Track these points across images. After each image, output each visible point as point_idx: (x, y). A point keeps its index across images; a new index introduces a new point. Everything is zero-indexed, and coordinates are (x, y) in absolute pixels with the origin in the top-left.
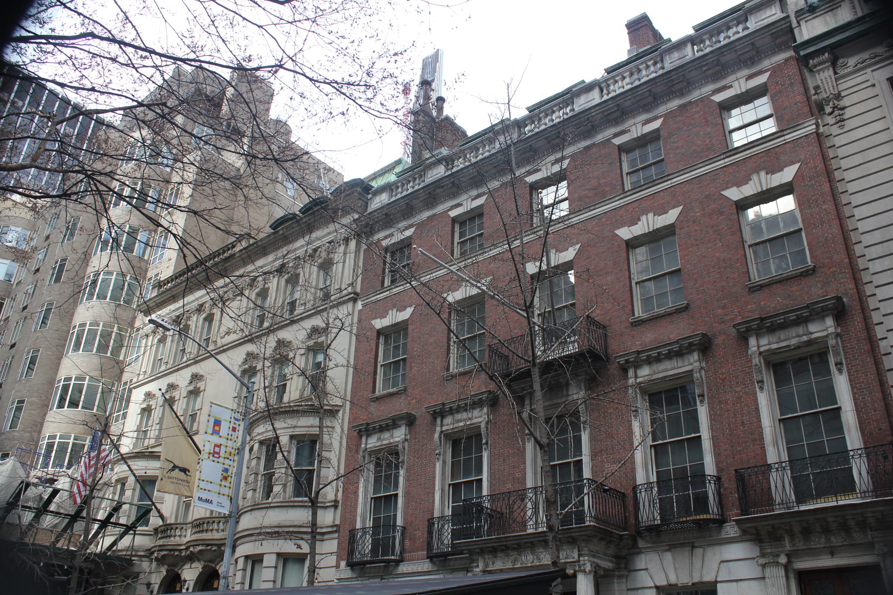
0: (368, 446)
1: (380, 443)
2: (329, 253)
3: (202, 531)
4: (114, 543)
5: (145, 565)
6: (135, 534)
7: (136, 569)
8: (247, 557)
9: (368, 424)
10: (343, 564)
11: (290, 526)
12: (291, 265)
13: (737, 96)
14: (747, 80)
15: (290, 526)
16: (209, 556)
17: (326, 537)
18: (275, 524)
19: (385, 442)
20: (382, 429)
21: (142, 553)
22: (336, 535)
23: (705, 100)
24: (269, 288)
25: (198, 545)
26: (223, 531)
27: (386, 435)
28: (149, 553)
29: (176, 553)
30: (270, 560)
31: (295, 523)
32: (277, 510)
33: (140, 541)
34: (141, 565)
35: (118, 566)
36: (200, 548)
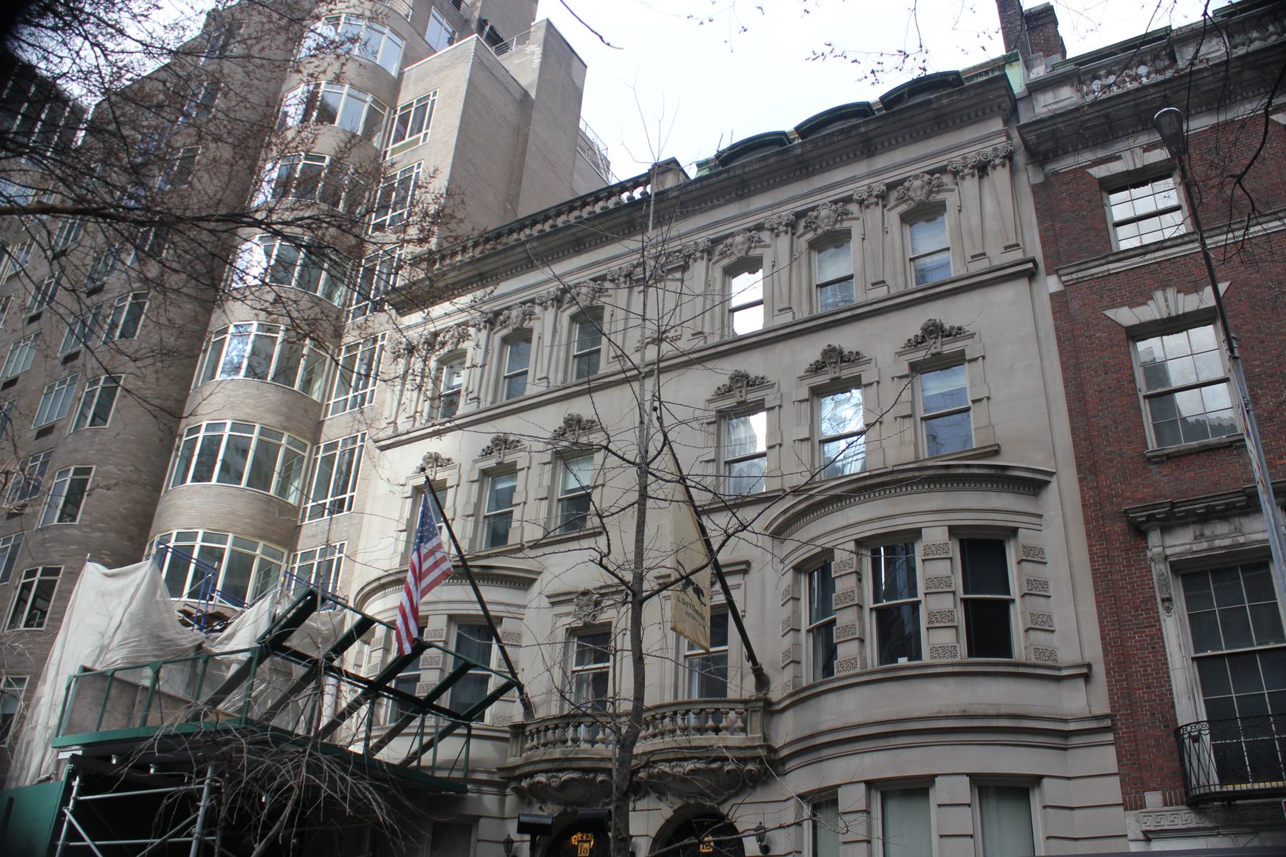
0: (1168, 552)
1: (1205, 545)
2: (930, 192)
3: (662, 734)
4: (416, 756)
5: (490, 802)
6: (469, 736)
7: (470, 810)
8: (870, 784)
9: (1173, 505)
12: (824, 213)
13: (1127, 173)
14: (1145, 151)
16: (700, 784)
17: (1075, 741)
18: (956, 710)
19: (1217, 543)
20: (1207, 517)
21: (484, 777)
22: (1110, 737)
23: (1081, 171)
24: (531, 331)
25: (685, 759)
26: (744, 730)
27: (1222, 528)
28: (507, 779)
29: (600, 778)
31: (1004, 711)
32: (950, 681)
33: (482, 751)
34: (479, 801)
36: (689, 766)
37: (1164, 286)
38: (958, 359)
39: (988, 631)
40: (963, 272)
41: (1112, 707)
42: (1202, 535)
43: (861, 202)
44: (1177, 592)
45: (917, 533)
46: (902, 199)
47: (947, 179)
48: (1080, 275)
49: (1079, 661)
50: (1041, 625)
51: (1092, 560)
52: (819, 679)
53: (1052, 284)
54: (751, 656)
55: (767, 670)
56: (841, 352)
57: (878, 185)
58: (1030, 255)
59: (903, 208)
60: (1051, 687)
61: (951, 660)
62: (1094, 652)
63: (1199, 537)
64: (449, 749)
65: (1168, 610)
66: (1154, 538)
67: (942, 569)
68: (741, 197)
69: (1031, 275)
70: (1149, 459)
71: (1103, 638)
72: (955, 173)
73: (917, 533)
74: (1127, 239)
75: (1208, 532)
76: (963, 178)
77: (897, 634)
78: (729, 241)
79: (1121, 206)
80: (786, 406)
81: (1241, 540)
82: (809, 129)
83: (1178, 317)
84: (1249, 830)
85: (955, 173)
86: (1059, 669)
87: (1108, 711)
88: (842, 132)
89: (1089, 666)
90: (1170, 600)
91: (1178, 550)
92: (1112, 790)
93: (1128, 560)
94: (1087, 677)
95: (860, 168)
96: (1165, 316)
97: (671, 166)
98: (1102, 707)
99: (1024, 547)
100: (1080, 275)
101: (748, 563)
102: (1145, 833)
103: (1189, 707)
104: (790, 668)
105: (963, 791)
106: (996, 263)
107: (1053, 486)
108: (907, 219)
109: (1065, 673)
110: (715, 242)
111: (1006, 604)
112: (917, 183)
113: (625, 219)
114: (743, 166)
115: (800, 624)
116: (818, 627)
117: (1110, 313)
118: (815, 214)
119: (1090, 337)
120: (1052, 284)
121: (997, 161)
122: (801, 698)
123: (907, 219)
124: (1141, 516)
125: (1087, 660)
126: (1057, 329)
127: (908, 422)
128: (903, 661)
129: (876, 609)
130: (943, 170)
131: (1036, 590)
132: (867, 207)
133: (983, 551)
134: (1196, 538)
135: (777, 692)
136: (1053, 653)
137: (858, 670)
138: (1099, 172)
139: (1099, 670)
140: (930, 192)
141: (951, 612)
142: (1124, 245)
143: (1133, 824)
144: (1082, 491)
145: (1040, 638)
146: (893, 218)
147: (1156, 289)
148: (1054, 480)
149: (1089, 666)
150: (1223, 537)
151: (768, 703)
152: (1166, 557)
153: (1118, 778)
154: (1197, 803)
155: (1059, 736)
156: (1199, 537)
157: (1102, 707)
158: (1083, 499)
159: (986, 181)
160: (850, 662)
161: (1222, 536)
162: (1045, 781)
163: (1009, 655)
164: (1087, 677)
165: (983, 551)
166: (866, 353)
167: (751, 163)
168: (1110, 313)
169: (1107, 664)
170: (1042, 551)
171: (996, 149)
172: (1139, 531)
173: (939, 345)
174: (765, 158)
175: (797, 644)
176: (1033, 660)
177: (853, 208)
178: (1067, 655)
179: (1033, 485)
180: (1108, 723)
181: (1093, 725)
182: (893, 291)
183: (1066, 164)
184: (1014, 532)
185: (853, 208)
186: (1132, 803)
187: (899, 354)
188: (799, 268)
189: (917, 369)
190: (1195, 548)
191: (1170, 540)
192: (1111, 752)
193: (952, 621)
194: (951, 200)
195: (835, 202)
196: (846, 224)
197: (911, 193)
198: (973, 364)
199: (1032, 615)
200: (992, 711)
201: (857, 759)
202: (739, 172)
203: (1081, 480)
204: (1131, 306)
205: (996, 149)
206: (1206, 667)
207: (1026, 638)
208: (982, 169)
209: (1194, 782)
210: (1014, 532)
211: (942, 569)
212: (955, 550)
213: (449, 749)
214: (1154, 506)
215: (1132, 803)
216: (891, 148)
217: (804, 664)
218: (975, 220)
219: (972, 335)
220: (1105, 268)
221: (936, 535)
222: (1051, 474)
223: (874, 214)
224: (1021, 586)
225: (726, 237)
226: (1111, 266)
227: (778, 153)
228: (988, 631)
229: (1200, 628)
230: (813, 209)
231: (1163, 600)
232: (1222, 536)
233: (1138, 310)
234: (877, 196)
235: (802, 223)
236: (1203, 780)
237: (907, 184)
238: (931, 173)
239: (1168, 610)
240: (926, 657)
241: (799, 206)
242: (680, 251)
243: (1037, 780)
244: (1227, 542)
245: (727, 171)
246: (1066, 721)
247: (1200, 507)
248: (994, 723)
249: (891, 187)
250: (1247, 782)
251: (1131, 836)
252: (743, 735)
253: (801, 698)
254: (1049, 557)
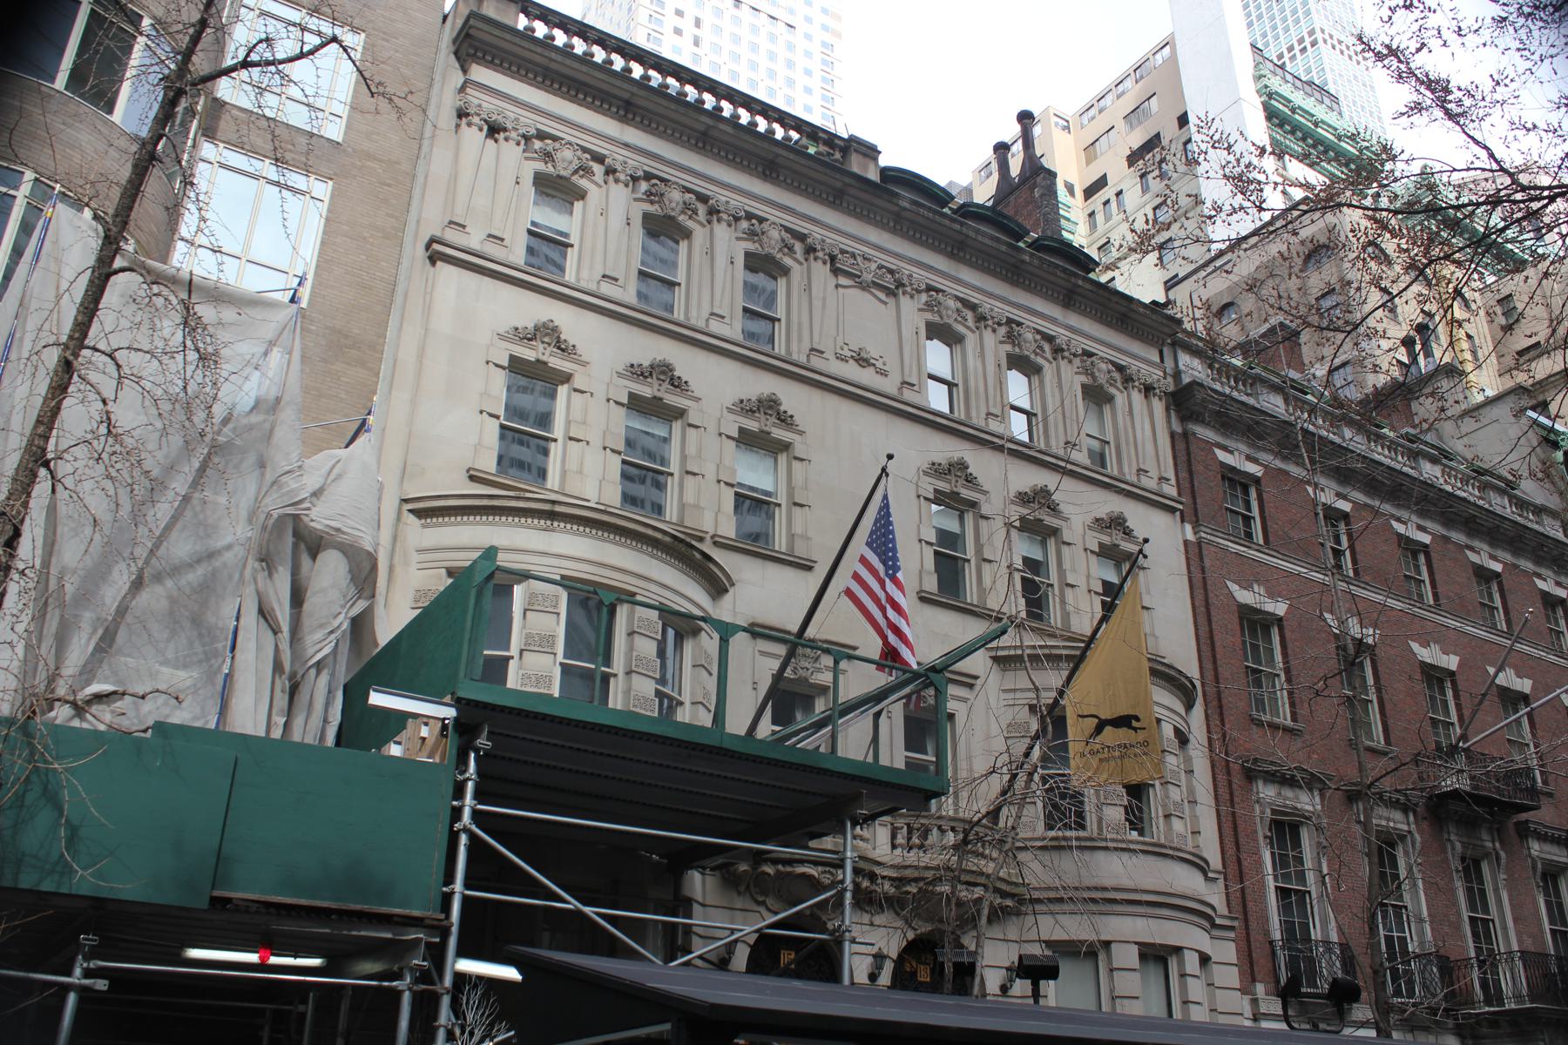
22: (1232, 935)
68: (952, 256)
85: (610, 171)
88: (1064, 270)
97: (871, 152)
101: (976, 678)
110: (929, 288)
112: (1103, 366)
113: (839, 185)
114: (977, 231)
138: (1222, 456)
167: (984, 234)
174: (998, 240)
183: (1204, 433)
201: (1129, 920)
202: (971, 234)
216: (1083, 312)
225: (938, 291)
227: (1010, 245)
242: (891, 272)
245: (962, 224)
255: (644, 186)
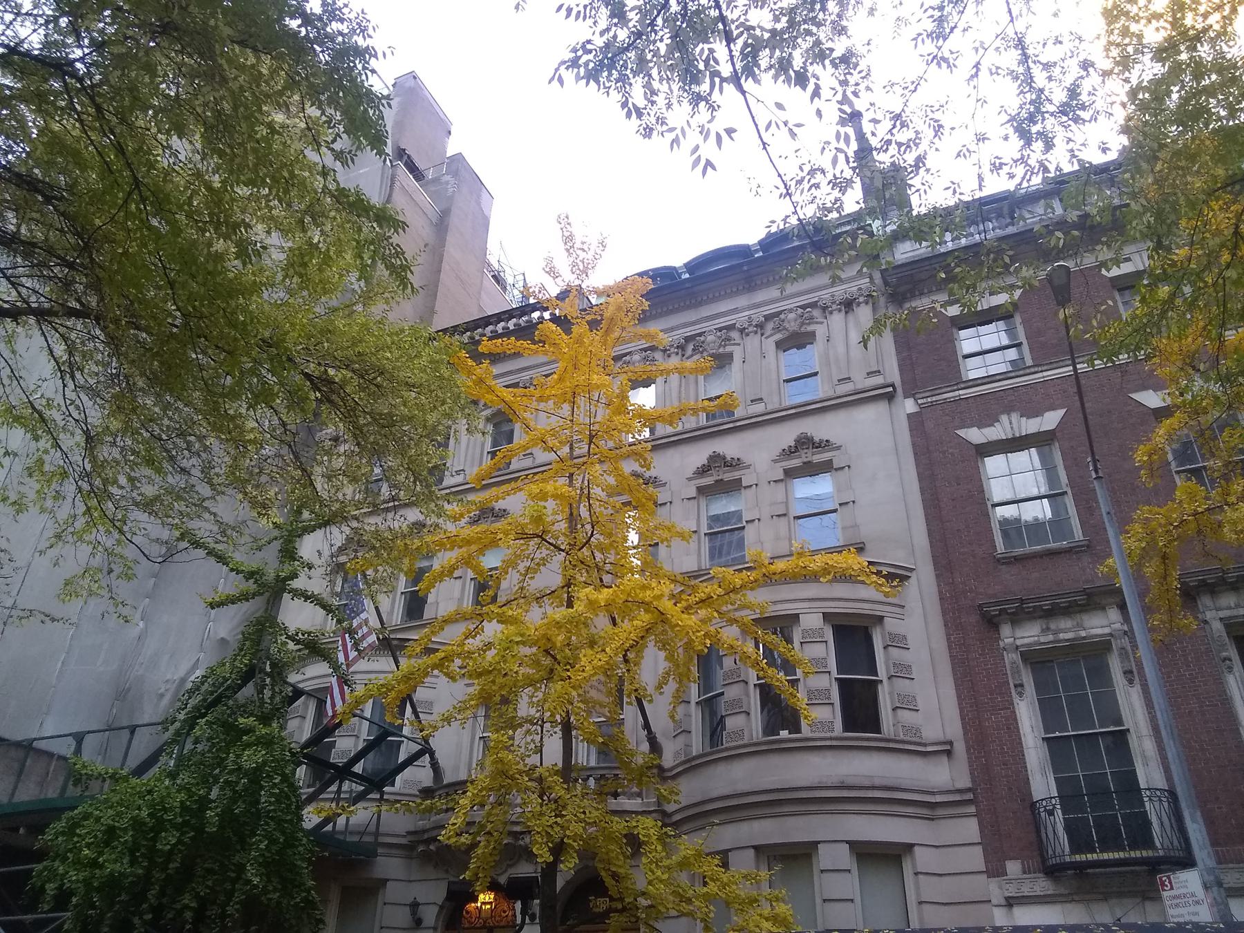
0: (1019, 642)
1: (1051, 638)
2: (802, 324)
10: (1013, 867)
11: (873, 788)
12: (710, 338)
15: (868, 788)
17: (941, 812)
19: (1062, 636)
20: (1051, 613)
22: (972, 809)
27: (1065, 623)
30: (834, 856)
31: (877, 782)
35: (346, 866)
37: (1008, 410)
38: (826, 467)
39: (860, 709)
40: (831, 394)
41: (973, 781)
42: (1048, 629)
43: (742, 331)
44: (1028, 679)
45: (795, 618)
46: (777, 329)
47: (816, 313)
48: (934, 399)
49: (942, 739)
50: (906, 703)
51: (950, 647)
52: (709, 750)
53: (910, 406)
54: (647, 725)
55: (660, 738)
56: (724, 458)
57: (758, 315)
58: (889, 381)
59: (778, 336)
60: (918, 762)
61: (828, 735)
62: (954, 729)
63: (1046, 630)
64: (362, 814)
65: (1021, 694)
66: (1006, 630)
67: (817, 651)
69: (890, 397)
70: (998, 560)
71: (963, 719)
72: (824, 309)
73: (795, 618)
74: (974, 370)
75: (1053, 626)
76: (831, 313)
77: (780, 713)
78: (628, 358)
79: (968, 341)
80: (677, 502)
81: (1083, 634)
82: (692, 266)
83: (1021, 437)
84: (1101, 897)
86: (925, 745)
87: (970, 785)
89: (951, 743)
90: (1022, 685)
91: (1026, 641)
92: (975, 858)
93: (983, 650)
94: (949, 753)
95: (742, 301)
96: (1010, 436)
98: (964, 782)
99: (890, 634)
100: (934, 399)
102: (1007, 899)
103: (1043, 785)
104: (681, 739)
105: (843, 856)
106: (860, 386)
107: (913, 581)
108: (782, 346)
109: (929, 749)
111: (874, 684)
112: (792, 316)
115: (689, 696)
116: (705, 700)
117: (961, 433)
118: (702, 338)
119: (944, 453)
120: (910, 406)
121: (861, 299)
122: (692, 766)
123: (779, 345)
124: (994, 610)
125: (949, 737)
126: (914, 445)
127: (783, 520)
128: (784, 734)
129: (760, 685)
130: (813, 305)
131: (901, 672)
132: (747, 335)
133: (853, 635)
134: (1043, 631)
135: (668, 760)
136: (918, 730)
137: (746, 741)
139: (960, 748)
140: (802, 324)
141: (828, 690)
142: (973, 375)
143: (995, 890)
144: (939, 586)
145: (905, 716)
146: (770, 344)
147: (1002, 413)
148: (913, 575)
149: (951, 743)
150: (1069, 630)
151: (661, 769)
152: (1017, 647)
153: (979, 849)
154: (1053, 871)
155: (929, 807)
156: (1046, 630)
157: (964, 782)
158: (940, 592)
159: (850, 316)
160: (739, 733)
161: (1066, 630)
162: (916, 848)
163: (878, 730)
164: (949, 753)
165: (853, 635)
166: (747, 459)
168: (961, 433)
169: (966, 742)
170: (905, 637)
171: (860, 289)
172: (991, 624)
173: (809, 455)
175: (688, 715)
176: (902, 737)
177: (735, 335)
178: (932, 732)
179: (897, 577)
180: (970, 796)
181: (957, 797)
182: (770, 408)
183: (922, 303)
184: (880, 620)
185: (735, 335)
186: (995, 870)
187: (775, 461)
188: (687, 384)
189: (790, 474)
190: (1042, 640)
191: (1019, 633)
192: (973, 824)
193: (829, 698)
194: (820, 331)
195: (720, 329)
196: (729, 349)
197: (786, 324)
198: (840, 472)
199: (899, 695)
200: (867, 783)
203: (937, 576)
204: (980, 426)
205: (860, 289)
206: (1054, 745)
207: (895, 716)
208: (848, 305)
209: (1050, 852)
210: (880, 620)
211: (817, 651)
212: (829, 635)
213: (362, 814)
214: (1007, 602)
215: (995, 870)
217: (694, 733)
218: (841, 349)
219: (839, 448)
220: (957, 393)
221: (812, 621)
222: (912, 570)
223: (753, 342)
224: (888, 670)
225: (625, 355)
226: (961, 392)
228: (860, 709)
229: (1049, 712)
230: (700, 335)
231: (1016, 686)
232: (1066, 630)
233: (987, 431)
234: (756, 326)
235: (690, 347)
236: (1058, 850)
237: (782, 316)
238: (803, 307)
239: (1021, 694)
240: (806, 731)
241: (689, 331)
243: (909, 847)
244: (1070, 635)
246: (933, 793)
247: (1046, 604)
248: (870, 794)
249: (768, 318)
250: (1093, 851)
251: (994, 901)
252: (639, 800)
253: (692, 766)
254: (911, 643)
255: (690, 347)
